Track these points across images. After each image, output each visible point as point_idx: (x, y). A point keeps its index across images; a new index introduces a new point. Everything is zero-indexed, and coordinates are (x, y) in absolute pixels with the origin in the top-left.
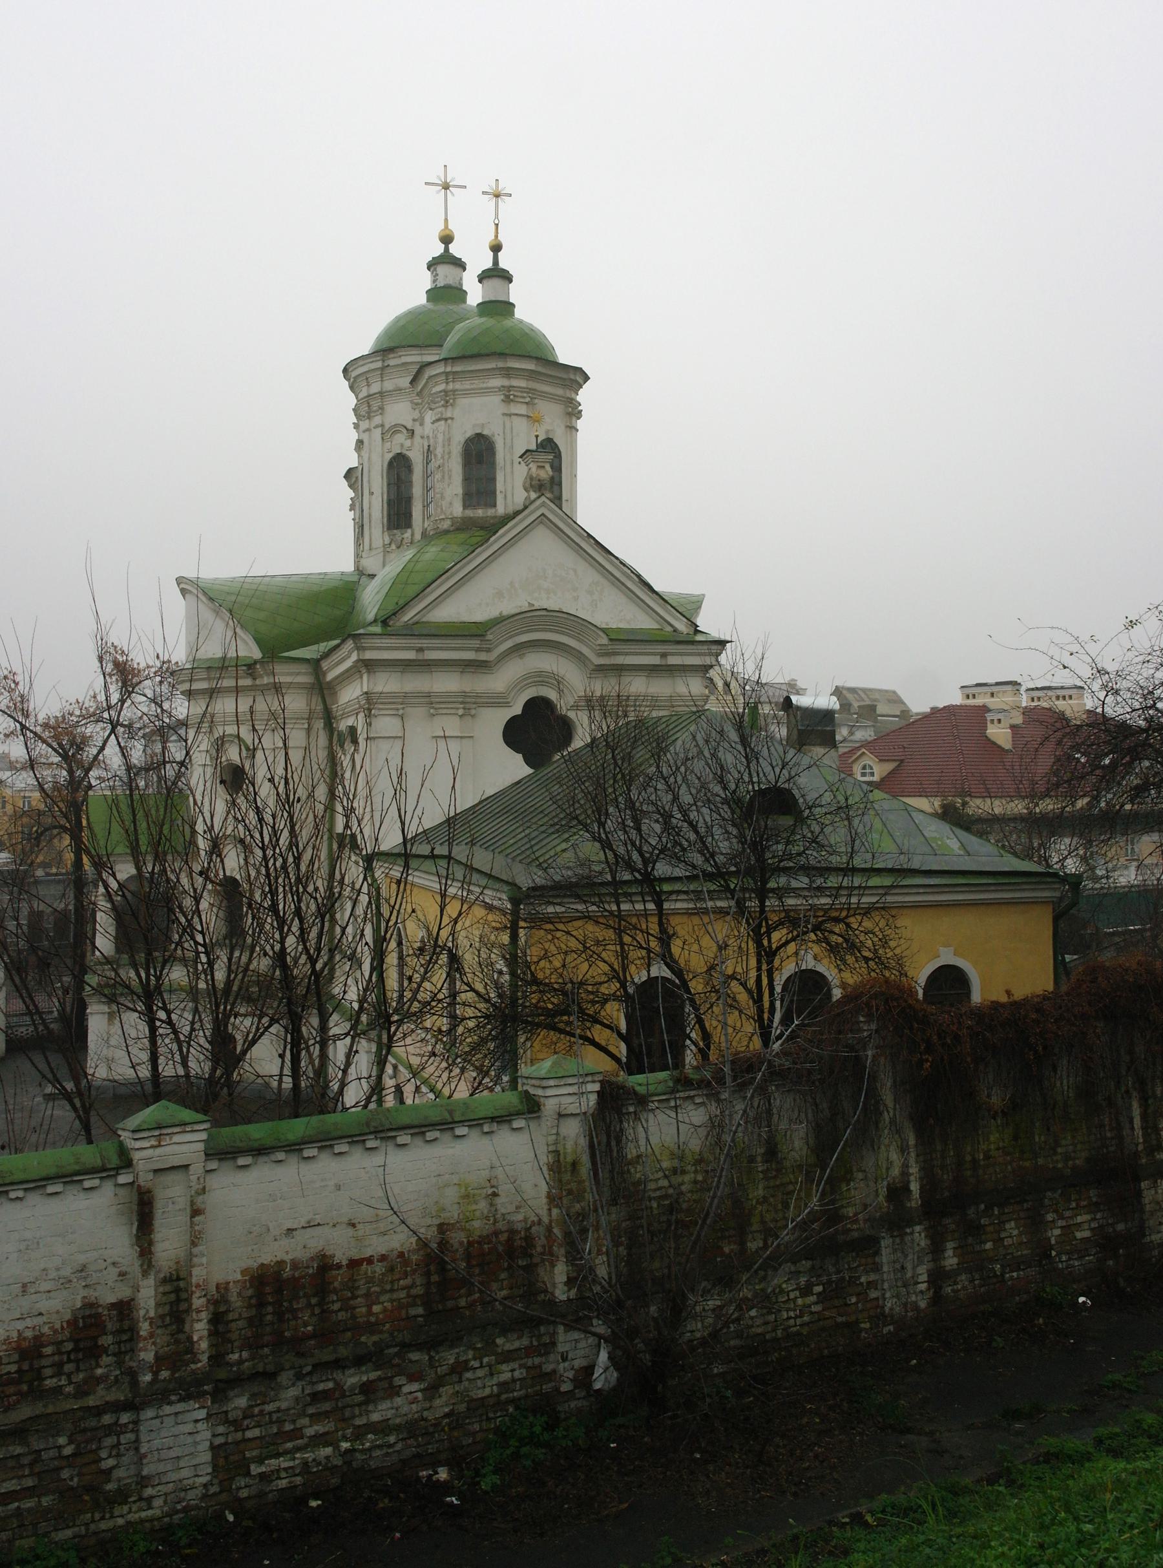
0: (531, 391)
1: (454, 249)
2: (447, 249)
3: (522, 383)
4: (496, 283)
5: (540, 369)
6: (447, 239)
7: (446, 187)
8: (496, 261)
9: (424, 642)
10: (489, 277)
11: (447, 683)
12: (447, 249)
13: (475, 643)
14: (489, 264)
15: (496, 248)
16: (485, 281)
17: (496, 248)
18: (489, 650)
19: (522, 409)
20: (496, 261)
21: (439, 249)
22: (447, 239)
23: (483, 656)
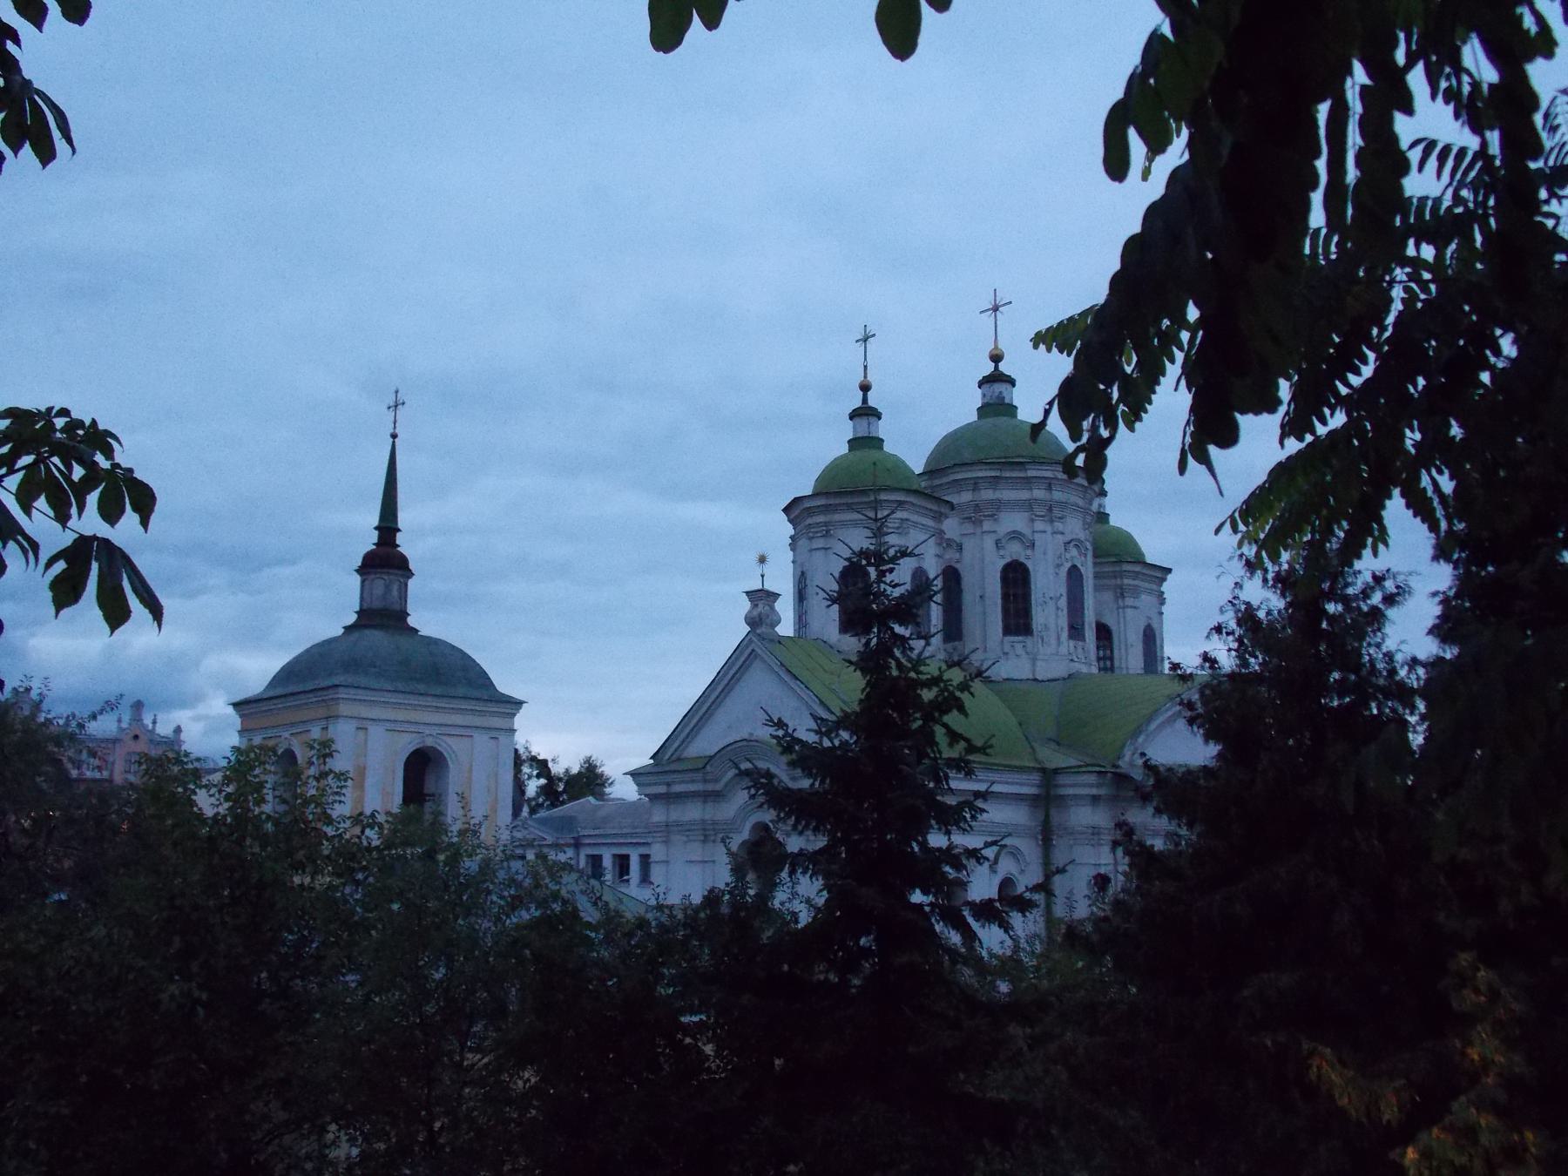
0: (826, 524)
1: (1003, 367)
2: (996, 368)
3: (821, 519)
4: (863, 422)
5: (832, 501)
6: (996, 358)
7: (996, 309)
8: (865, 400)
9: (669, 778)
10: (860, 415)
11: (693, 812)
12: (996, 368)
13: (699, 776)
14: (858, 403)
15: (865, 388)
16: (857, 420)
17: (865, 388)
18: (716, 781)
19: (820, 543)
20: (865, 400)
21: (989, 368)
22: (996, 358)
23: (710, 787)
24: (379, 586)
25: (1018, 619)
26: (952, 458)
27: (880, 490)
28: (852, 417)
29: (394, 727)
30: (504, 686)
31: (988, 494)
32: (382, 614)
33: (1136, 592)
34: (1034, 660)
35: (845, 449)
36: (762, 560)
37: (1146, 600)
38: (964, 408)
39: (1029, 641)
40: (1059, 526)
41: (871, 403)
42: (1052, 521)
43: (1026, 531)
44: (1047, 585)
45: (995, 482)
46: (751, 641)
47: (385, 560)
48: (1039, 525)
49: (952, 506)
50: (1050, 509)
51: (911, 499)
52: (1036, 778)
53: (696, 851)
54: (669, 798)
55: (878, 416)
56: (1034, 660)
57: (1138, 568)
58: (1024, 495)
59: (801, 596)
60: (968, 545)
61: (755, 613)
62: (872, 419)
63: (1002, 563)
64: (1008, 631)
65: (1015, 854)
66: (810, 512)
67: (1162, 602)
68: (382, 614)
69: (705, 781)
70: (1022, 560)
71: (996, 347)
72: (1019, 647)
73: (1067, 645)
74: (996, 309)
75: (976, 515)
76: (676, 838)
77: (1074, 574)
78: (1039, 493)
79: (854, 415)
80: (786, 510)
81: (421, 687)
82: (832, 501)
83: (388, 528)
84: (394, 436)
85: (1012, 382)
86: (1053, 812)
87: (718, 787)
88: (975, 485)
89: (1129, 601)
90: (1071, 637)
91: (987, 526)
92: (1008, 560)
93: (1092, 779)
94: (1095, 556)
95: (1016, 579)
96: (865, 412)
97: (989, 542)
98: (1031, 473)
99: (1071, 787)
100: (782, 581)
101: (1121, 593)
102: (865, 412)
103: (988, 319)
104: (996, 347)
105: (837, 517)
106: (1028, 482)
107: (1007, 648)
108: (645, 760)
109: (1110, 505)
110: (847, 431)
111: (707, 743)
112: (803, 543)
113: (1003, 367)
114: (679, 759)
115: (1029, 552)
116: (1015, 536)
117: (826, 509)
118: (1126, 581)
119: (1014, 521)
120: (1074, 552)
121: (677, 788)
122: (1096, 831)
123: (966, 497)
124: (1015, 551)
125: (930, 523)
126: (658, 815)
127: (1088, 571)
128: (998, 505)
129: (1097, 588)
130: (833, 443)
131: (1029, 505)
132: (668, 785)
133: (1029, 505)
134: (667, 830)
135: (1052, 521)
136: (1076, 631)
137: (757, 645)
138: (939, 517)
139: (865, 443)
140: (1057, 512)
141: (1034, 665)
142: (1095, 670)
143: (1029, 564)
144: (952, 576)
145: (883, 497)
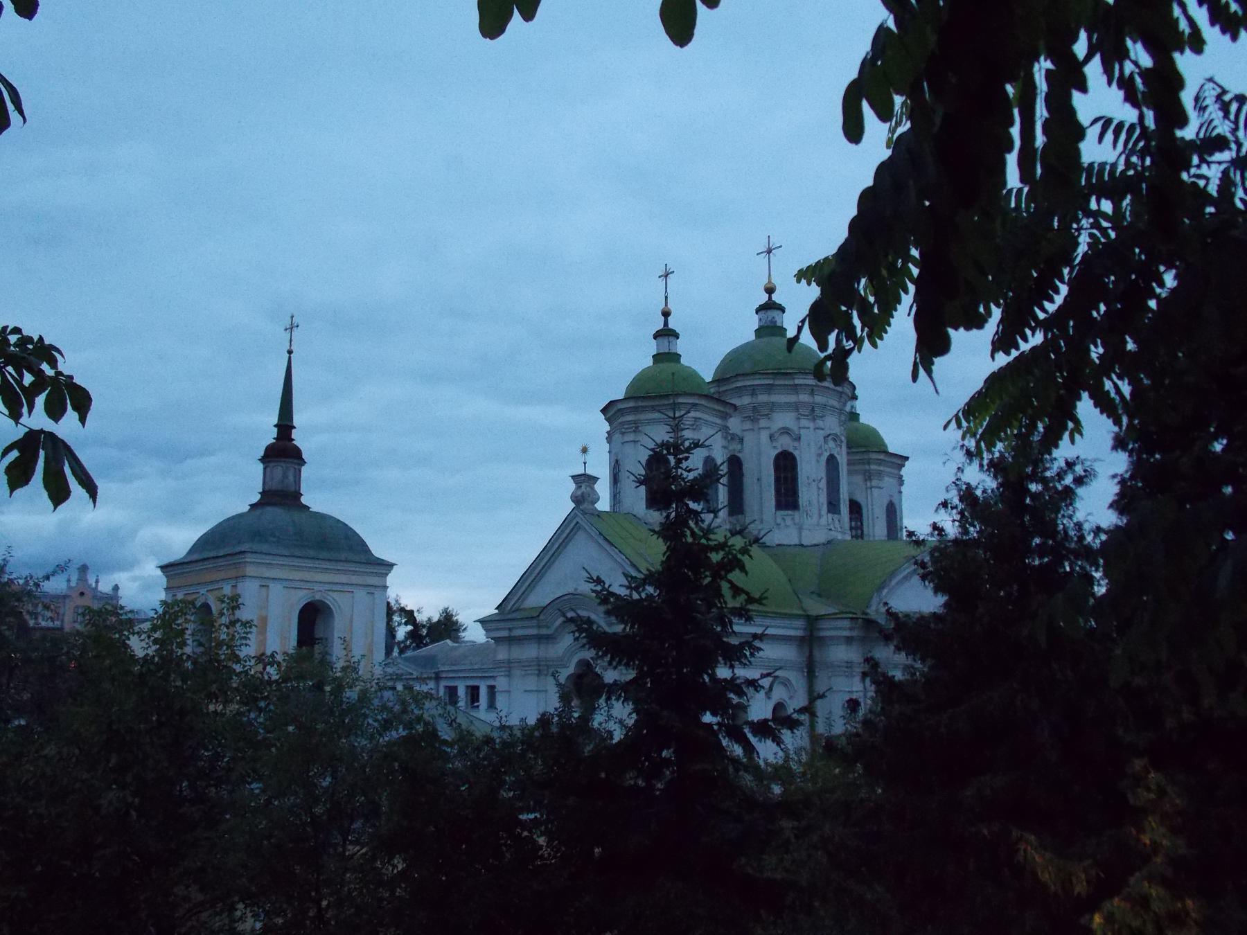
0: (635, 422)
1: (775, 297)
2: (770, 298)
3: (630, 418)
4: (664, 341)
5: (640, 404)
6: (770, 290)
7: (769, 251)
8: (666, 324)
9: (509, 625)
11: (530, 652)
12: (770, 298)
13: (534, 622)
15: (666, 314)
16: (660, 339)
17: (666, 314)
19: (631, 437)
20: (666, 324)
21: (765, 297)
22: (770, 290)
23: (544, 631)
24: (278, 471)
25: (787, 497)
26: (735, 369)
27: (677, 395)
28: (656, 336)
29: (290, 584)
30: (378, 550)
31: (763, 398)
32: (281, 495)
33: (880, 474)
34: (800, 529)
35: (650, 362)
36: (585, 450)
37: (888, 482)
38: (745, 330)
39: (796, 514)
40: (820, 423)
41: (671, 326)
42: (814, 419)
43: (795, 429)
44: (810, 471)
45: (769, 389)
46: (576, 515)
47: (283, 451)
48: (804, 423)
49: (735, 407)
50: (813, 410)
51: (703, 402)
52: (800, 623)
53: (532, 682)
54: (511, 640)
55: (677, 336)
56: (800, 529)
57: (882, 457)
58: (792, 398)
59: (615, 479)
60: (749, 439)
61: (579, 493)
62: (671, 339)
63: (774, 453)
64: (780, 506)
65: (786, 683)
66: (622, 412)
67: (901, 481)
68: (281, 495)
69: (539, 627)
70: (791, 450)
71: (770, 282)
72: (789, 522)
73: (826, 518)
74: (769, 251)
75: (755, 415)
76: (517, 672)
77: (832, 461)
78: (804, 398)
79: (657, 336)
80: (604, 411)
81: (312, 553)
82: (640, 404)
83: (285, 426)
84: (290, 352)
85: (782, 310)
86: (816, 654)
87: (550, 632)
88: (753, 391)
89: (875, 483)
90: (829, 511)
91: (763, 423)
92: (780, 450)
93: (847, 623)
94: (849, 447)
95: (786, 465)
96: (666, 333)
97: (764, 436)
98: (797, 382)
99: (828, 630)
100: (600, 468)
101: (868, 476)
102: (666, 333)
103: (763, 259)
104: (770, 282)
105: (643, 417)
106: (796, 388)
107: (779, 520)
108: (490, 610)
109: (860, 406)
110: (652, 348)
111: (540, 597)
112: (617, 436)
113: (775, 297)
114: (518, 610)
115: (796, 444)
116: (786, 431)
117: (635, 410)
118: (873, 467)
119: (784, 419)
120: (831, 444)
121: (518, 633)
122: (849, 665)
123: (746, 400)
124: (785, 443)
125: (719, 421)
126: (502, 654)
127: (842, 459)
128: (772, 407)
129: (850, 473)
130: (640, 358)
131: (796, 407)
132: (510, 629)
133: (796, 407)
134: (508, 667)
135: (814, 419)
136: (833, 507)
137: (580, 518)
138: (725, 416)
139: (666, 358)
140: (817, 412)
141: (800, 533)
142: (849, 538)
143: (796, 453)
144: (735, 463)
145: (680, 400)
